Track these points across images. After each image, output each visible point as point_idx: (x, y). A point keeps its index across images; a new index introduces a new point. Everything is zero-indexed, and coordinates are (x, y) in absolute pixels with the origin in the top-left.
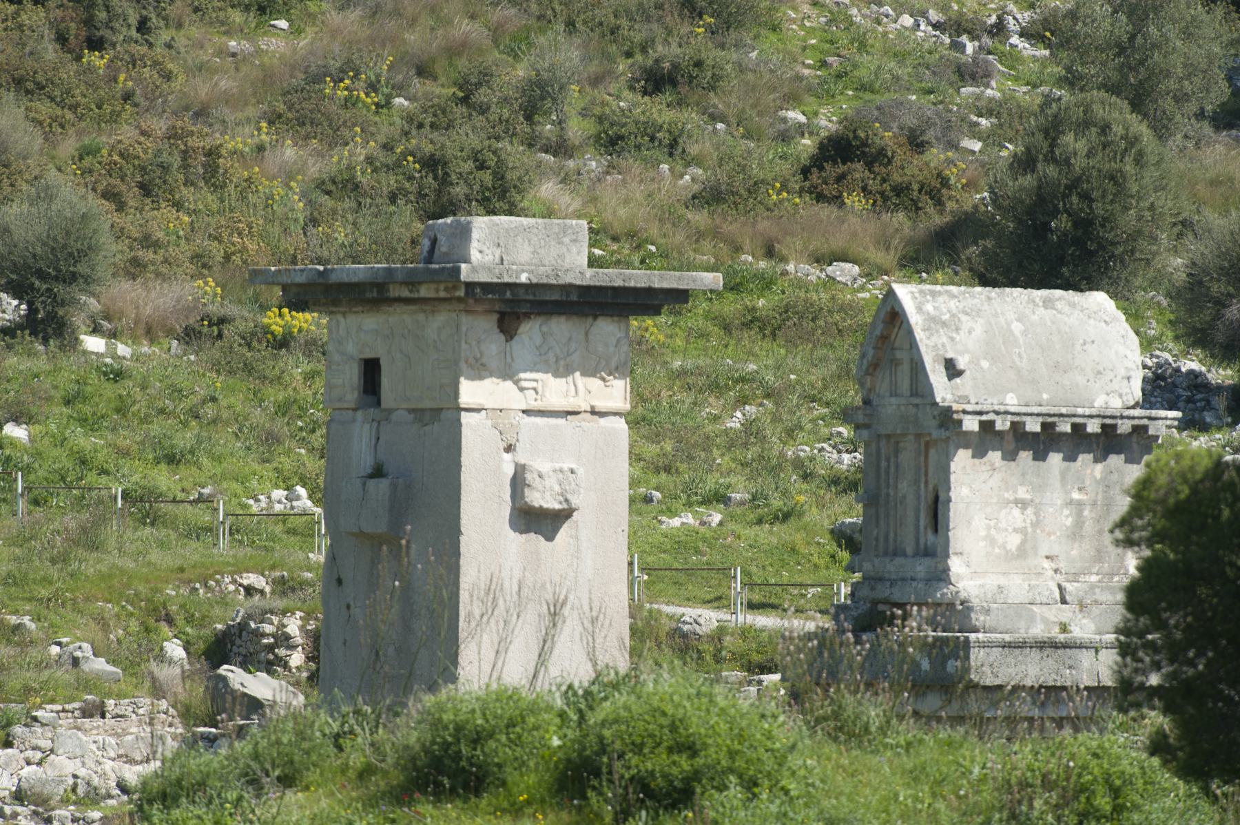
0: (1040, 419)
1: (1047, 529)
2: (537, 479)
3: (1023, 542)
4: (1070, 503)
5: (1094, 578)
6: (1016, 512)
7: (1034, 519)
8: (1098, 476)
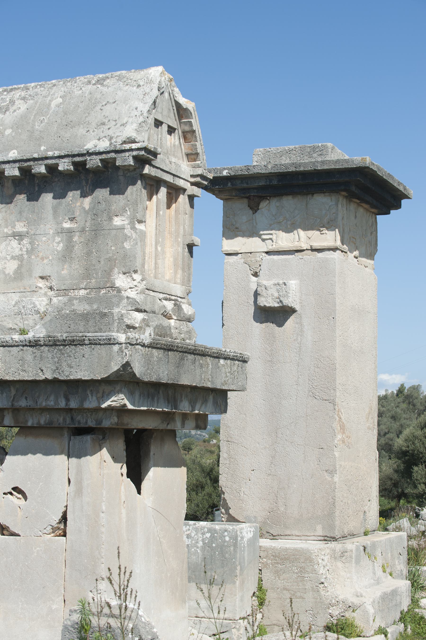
0: (17, 165)
1: (41, 255)
2: (264, 290)
3: (20, 267)
4: (61, 231)
5: (82, 292)
6: (14, 243)
7: (29, 246)
8: (87, 207)
